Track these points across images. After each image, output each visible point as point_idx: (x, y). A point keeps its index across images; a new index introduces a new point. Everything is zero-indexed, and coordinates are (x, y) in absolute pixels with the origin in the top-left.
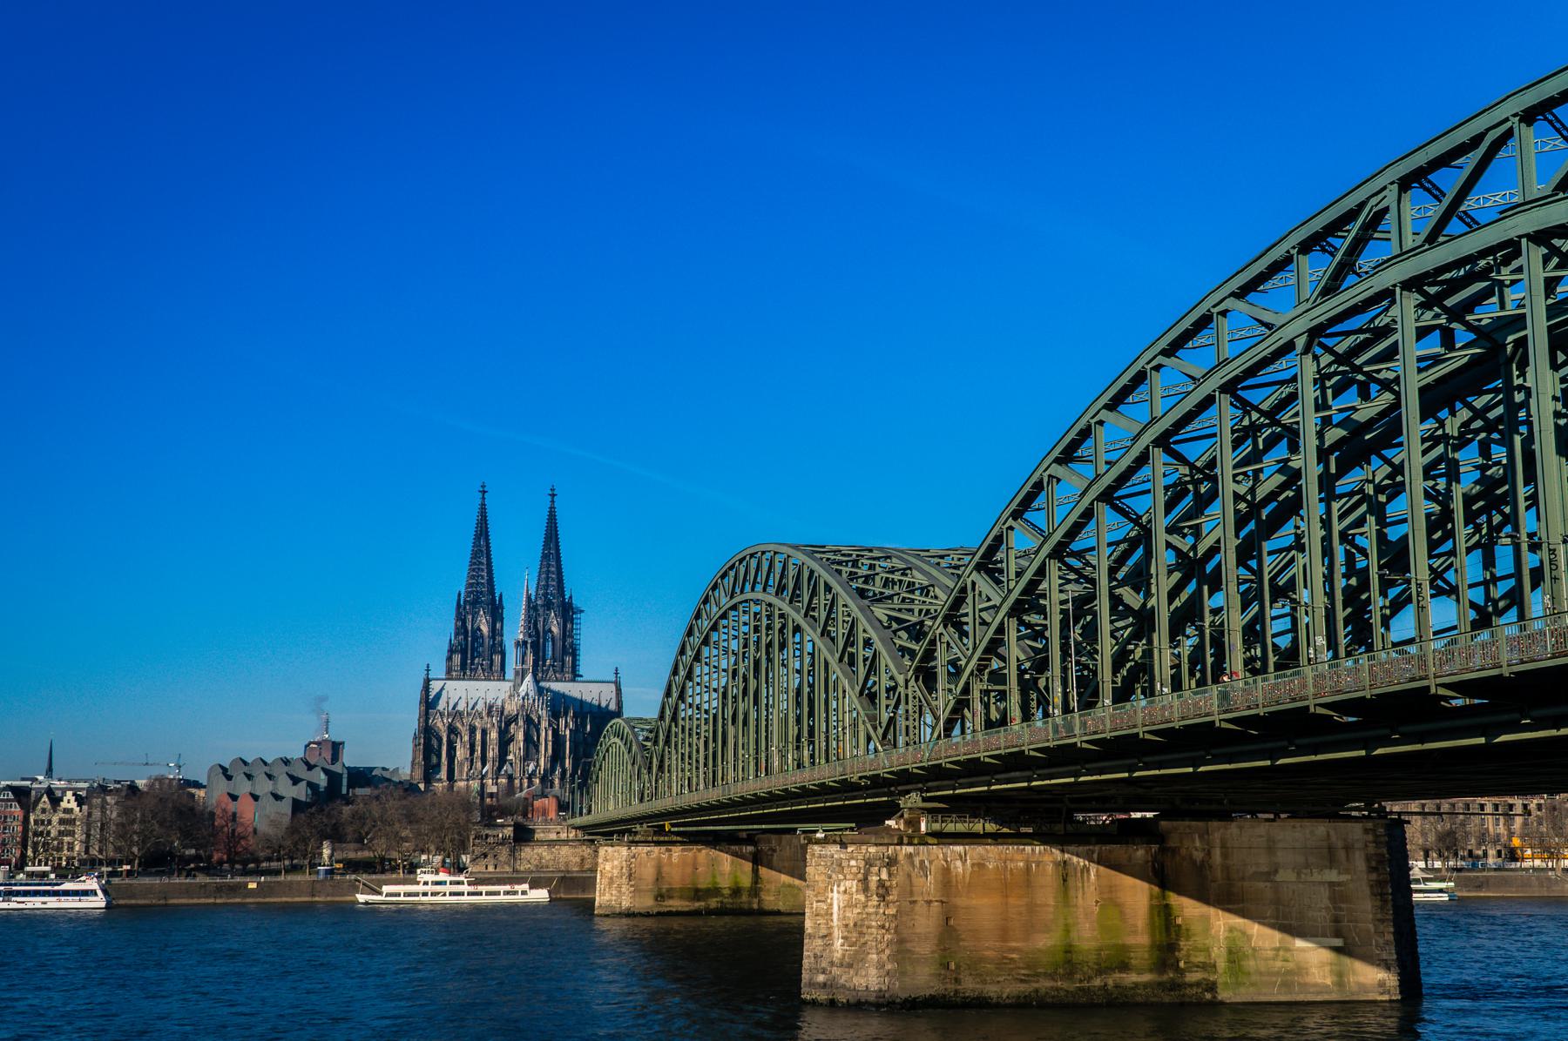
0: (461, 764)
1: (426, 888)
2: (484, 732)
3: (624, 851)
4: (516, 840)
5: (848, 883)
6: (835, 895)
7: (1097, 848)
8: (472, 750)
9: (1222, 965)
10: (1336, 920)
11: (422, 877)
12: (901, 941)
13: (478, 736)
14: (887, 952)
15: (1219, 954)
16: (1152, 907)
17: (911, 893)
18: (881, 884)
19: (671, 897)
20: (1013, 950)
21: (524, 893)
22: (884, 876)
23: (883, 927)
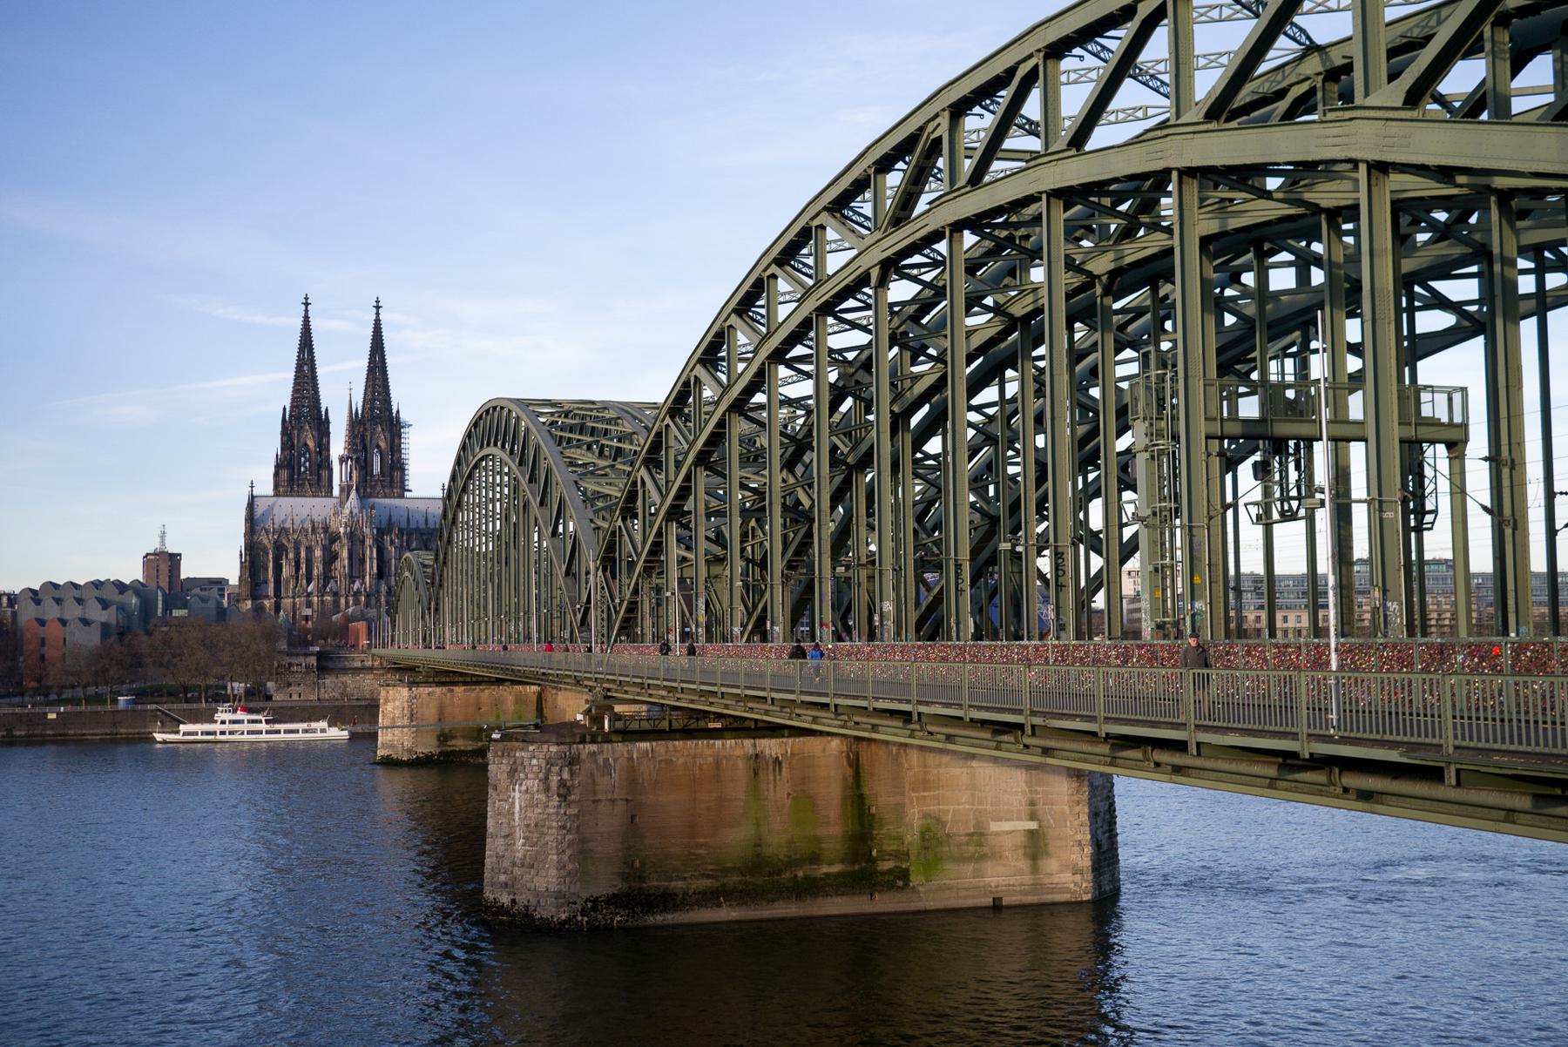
0: (287, 582)
1: (224, 727)
2: (309, 550)
3: (405, 692)
4: (319, 668)
5: (530, 783)
6: (517, 795)
7: (790, 740)
9: (914, 852)
10: (1032, 803)
11: (219, 716)
12: (583, 841)
13: (303, 554)
14: (569, 852)
15: (912, 837)
16: (844, 799)
17: (595, 793)
18: (562, 783)
19: (453, 737)
20: (702, 846)
21: (323, 731)
22: (566, 776)
23: (564, 827)
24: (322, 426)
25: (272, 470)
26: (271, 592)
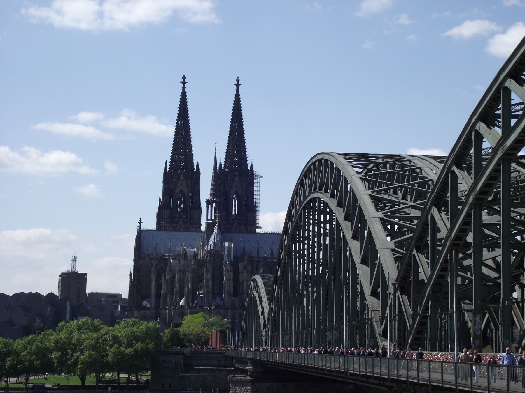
0: (165, 297)
24: (194, 176)
25: (156, 210)
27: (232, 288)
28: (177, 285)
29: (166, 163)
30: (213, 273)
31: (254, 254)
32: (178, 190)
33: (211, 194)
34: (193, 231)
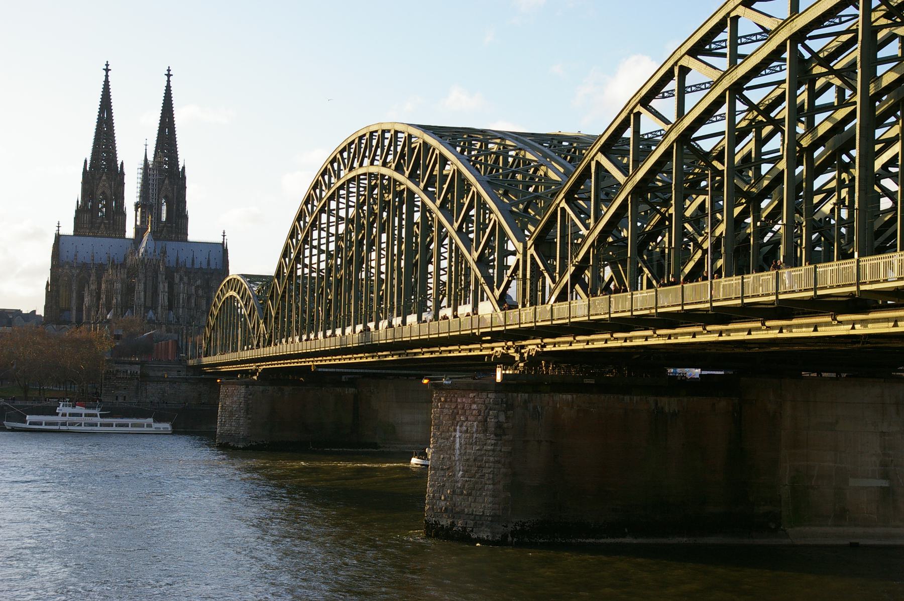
8: (99, 298)
11: (61, 409)
18: (499, 425)
21: (149, 426)
22: (502, 418)
24: (117, 176)
25: (73, 214)
26: (74, 320)
27: (166, 300)
28: (103, 296)
29: (86, 161)
30: (145, 284)
31: (189, 265)
32: (99, 192)
33: (140, 196)
34: (115, 237)
